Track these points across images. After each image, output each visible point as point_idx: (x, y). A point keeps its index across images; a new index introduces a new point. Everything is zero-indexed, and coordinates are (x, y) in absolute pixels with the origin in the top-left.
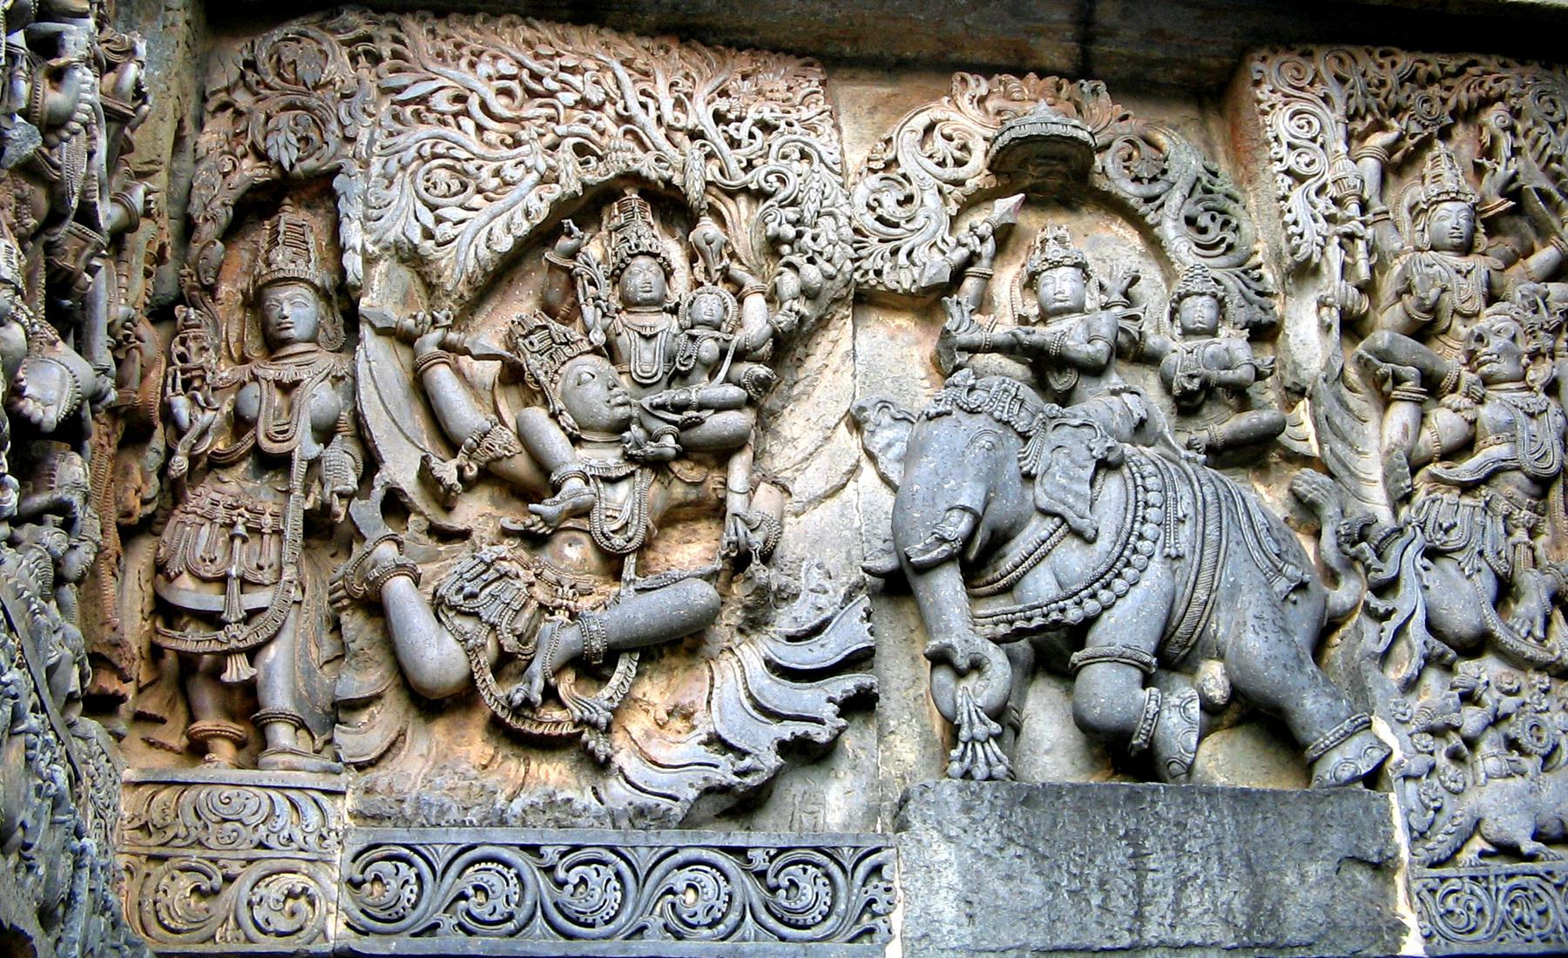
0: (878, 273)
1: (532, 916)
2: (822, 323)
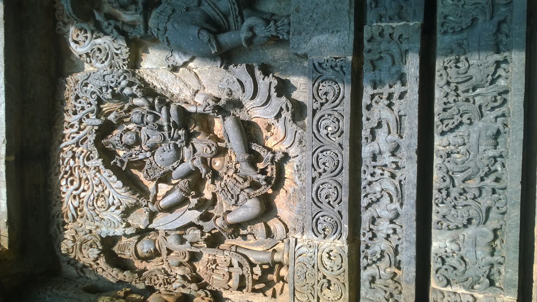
0: (124, 60)
2: (142, 80)
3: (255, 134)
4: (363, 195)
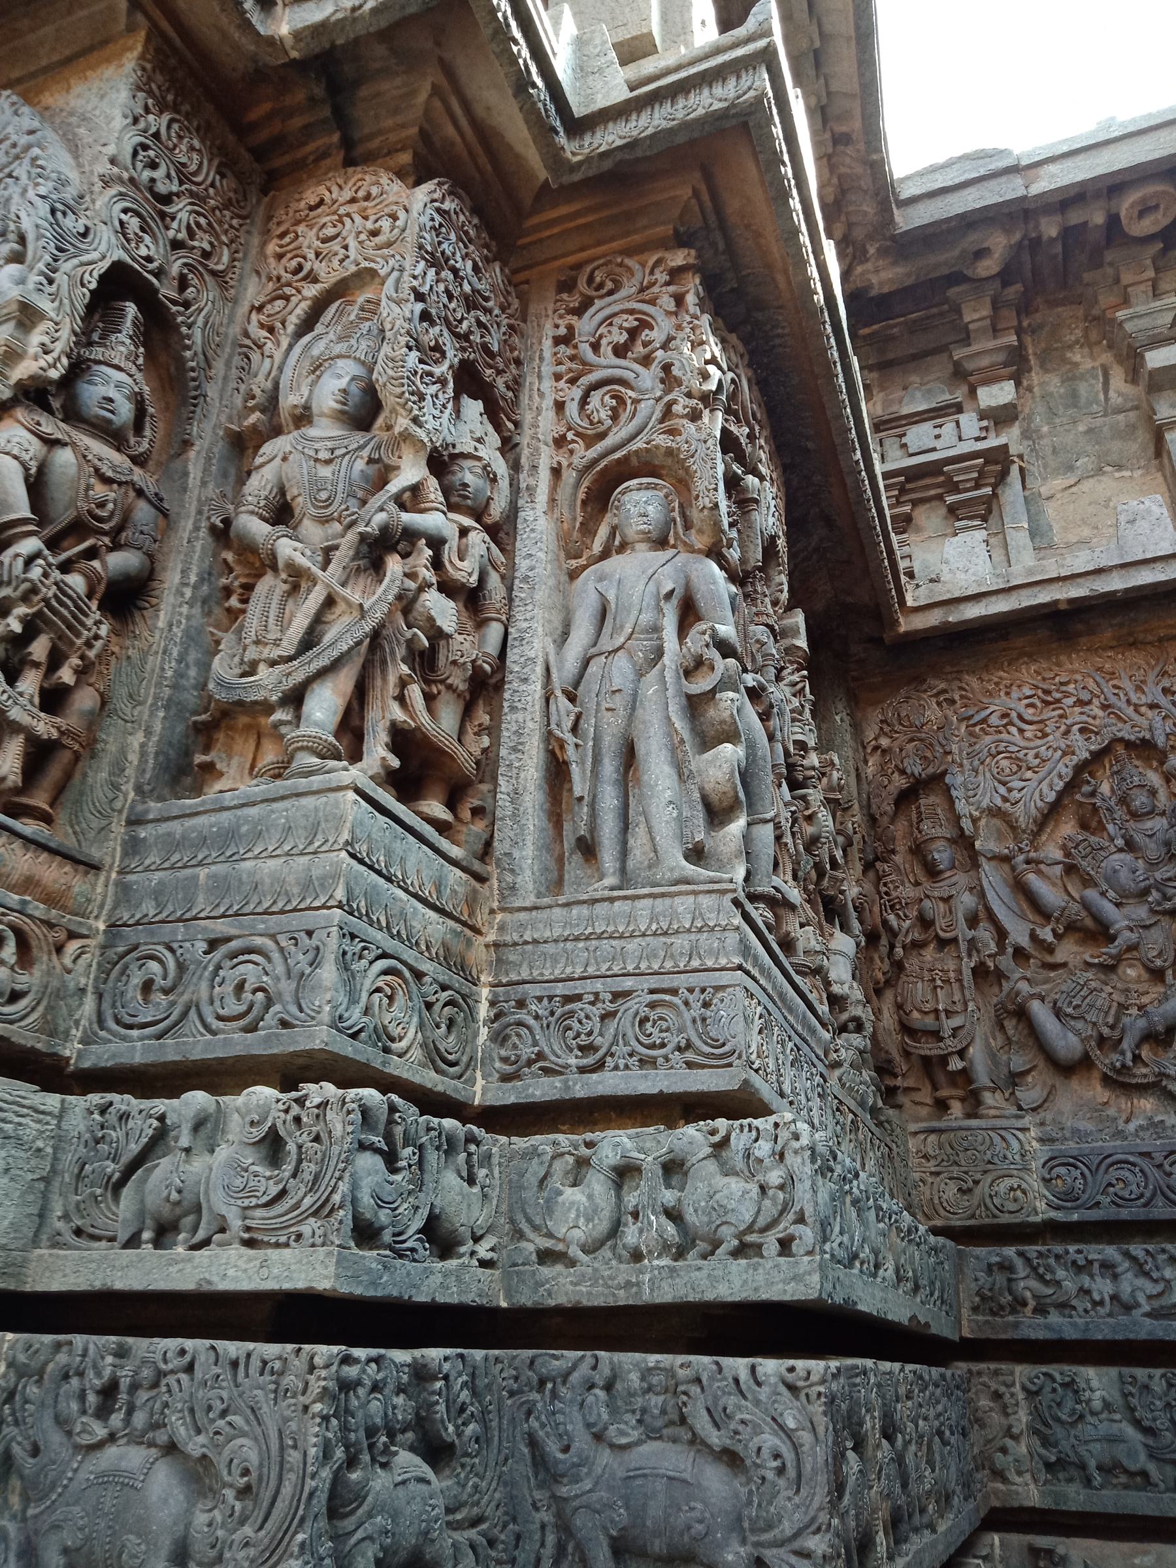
4: (1150, 1247)
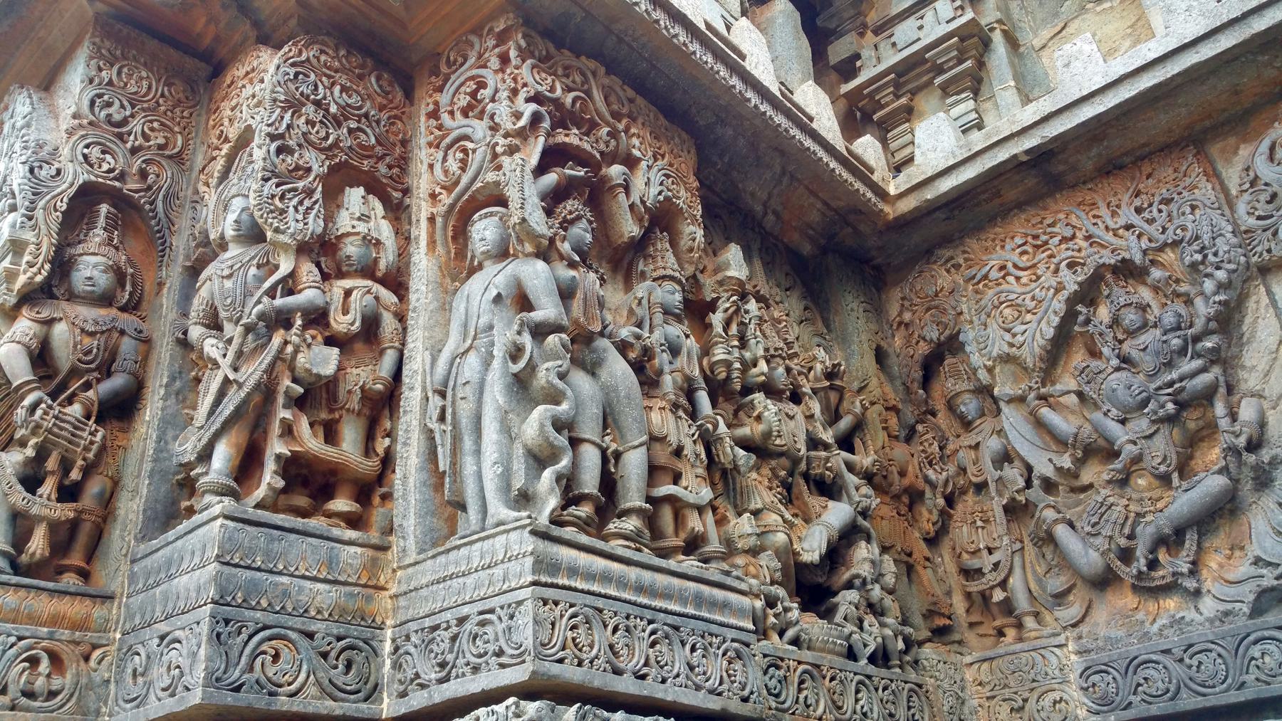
1: (1179, 688)
3: (1217, 528)
